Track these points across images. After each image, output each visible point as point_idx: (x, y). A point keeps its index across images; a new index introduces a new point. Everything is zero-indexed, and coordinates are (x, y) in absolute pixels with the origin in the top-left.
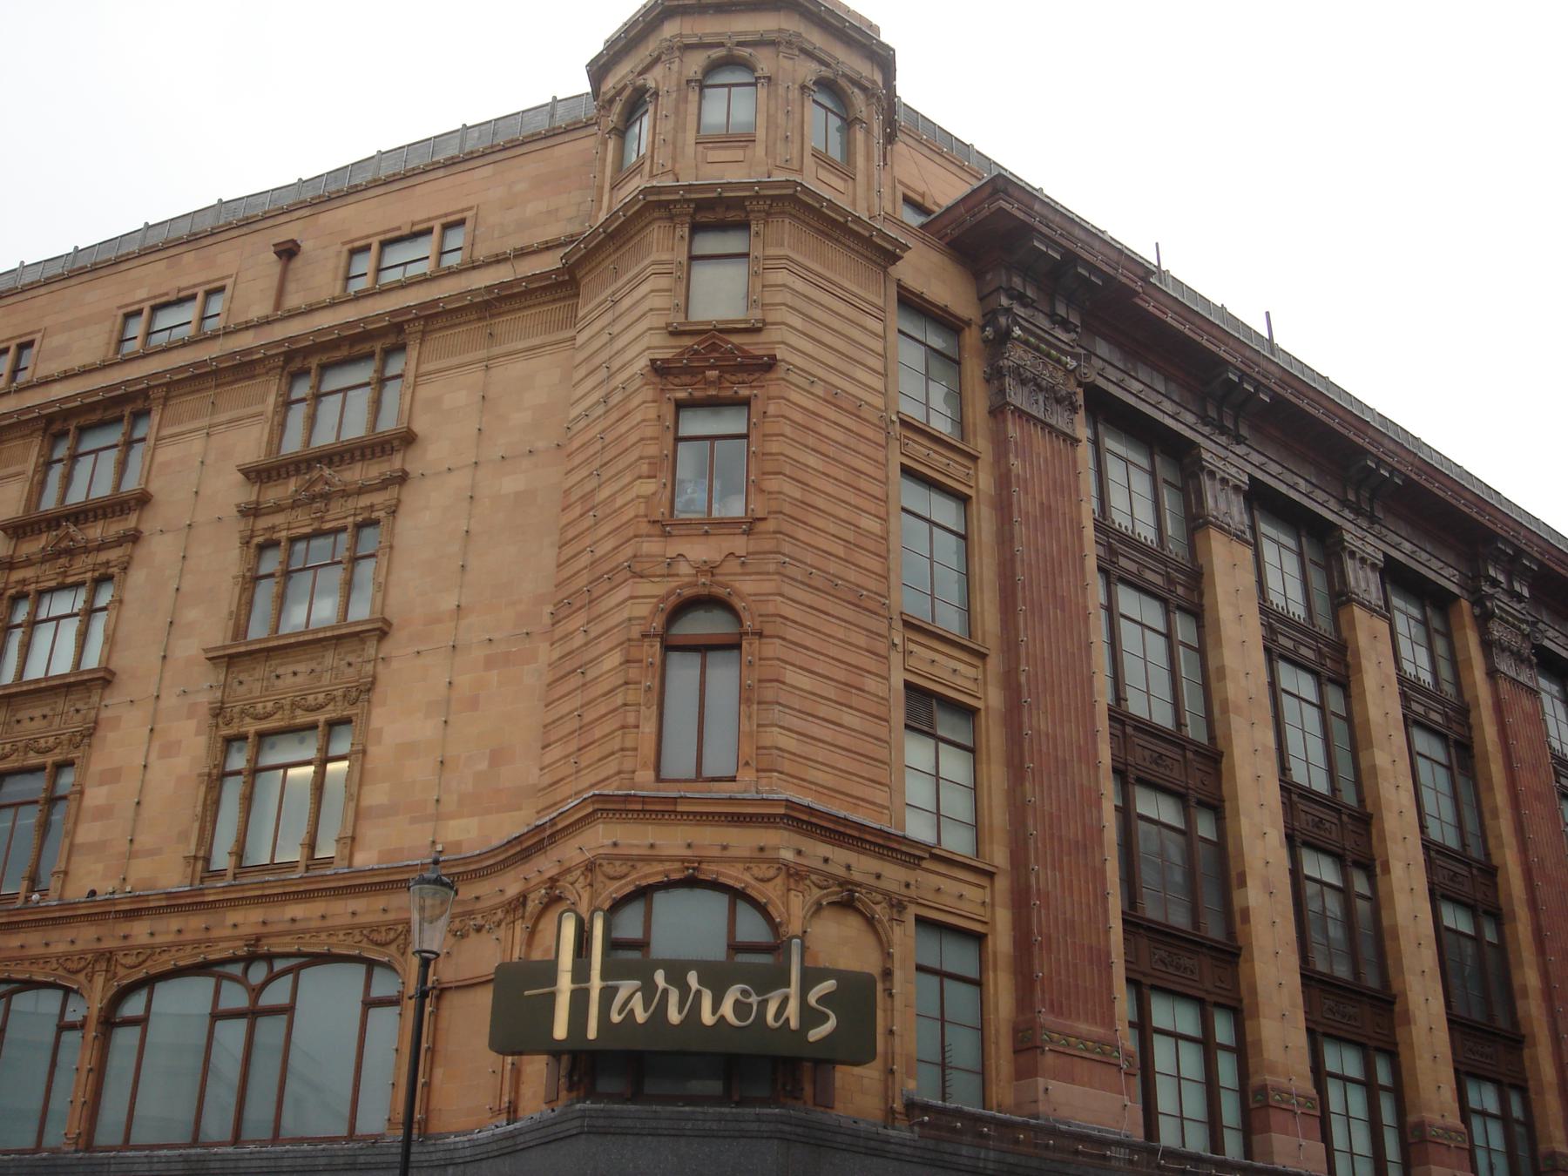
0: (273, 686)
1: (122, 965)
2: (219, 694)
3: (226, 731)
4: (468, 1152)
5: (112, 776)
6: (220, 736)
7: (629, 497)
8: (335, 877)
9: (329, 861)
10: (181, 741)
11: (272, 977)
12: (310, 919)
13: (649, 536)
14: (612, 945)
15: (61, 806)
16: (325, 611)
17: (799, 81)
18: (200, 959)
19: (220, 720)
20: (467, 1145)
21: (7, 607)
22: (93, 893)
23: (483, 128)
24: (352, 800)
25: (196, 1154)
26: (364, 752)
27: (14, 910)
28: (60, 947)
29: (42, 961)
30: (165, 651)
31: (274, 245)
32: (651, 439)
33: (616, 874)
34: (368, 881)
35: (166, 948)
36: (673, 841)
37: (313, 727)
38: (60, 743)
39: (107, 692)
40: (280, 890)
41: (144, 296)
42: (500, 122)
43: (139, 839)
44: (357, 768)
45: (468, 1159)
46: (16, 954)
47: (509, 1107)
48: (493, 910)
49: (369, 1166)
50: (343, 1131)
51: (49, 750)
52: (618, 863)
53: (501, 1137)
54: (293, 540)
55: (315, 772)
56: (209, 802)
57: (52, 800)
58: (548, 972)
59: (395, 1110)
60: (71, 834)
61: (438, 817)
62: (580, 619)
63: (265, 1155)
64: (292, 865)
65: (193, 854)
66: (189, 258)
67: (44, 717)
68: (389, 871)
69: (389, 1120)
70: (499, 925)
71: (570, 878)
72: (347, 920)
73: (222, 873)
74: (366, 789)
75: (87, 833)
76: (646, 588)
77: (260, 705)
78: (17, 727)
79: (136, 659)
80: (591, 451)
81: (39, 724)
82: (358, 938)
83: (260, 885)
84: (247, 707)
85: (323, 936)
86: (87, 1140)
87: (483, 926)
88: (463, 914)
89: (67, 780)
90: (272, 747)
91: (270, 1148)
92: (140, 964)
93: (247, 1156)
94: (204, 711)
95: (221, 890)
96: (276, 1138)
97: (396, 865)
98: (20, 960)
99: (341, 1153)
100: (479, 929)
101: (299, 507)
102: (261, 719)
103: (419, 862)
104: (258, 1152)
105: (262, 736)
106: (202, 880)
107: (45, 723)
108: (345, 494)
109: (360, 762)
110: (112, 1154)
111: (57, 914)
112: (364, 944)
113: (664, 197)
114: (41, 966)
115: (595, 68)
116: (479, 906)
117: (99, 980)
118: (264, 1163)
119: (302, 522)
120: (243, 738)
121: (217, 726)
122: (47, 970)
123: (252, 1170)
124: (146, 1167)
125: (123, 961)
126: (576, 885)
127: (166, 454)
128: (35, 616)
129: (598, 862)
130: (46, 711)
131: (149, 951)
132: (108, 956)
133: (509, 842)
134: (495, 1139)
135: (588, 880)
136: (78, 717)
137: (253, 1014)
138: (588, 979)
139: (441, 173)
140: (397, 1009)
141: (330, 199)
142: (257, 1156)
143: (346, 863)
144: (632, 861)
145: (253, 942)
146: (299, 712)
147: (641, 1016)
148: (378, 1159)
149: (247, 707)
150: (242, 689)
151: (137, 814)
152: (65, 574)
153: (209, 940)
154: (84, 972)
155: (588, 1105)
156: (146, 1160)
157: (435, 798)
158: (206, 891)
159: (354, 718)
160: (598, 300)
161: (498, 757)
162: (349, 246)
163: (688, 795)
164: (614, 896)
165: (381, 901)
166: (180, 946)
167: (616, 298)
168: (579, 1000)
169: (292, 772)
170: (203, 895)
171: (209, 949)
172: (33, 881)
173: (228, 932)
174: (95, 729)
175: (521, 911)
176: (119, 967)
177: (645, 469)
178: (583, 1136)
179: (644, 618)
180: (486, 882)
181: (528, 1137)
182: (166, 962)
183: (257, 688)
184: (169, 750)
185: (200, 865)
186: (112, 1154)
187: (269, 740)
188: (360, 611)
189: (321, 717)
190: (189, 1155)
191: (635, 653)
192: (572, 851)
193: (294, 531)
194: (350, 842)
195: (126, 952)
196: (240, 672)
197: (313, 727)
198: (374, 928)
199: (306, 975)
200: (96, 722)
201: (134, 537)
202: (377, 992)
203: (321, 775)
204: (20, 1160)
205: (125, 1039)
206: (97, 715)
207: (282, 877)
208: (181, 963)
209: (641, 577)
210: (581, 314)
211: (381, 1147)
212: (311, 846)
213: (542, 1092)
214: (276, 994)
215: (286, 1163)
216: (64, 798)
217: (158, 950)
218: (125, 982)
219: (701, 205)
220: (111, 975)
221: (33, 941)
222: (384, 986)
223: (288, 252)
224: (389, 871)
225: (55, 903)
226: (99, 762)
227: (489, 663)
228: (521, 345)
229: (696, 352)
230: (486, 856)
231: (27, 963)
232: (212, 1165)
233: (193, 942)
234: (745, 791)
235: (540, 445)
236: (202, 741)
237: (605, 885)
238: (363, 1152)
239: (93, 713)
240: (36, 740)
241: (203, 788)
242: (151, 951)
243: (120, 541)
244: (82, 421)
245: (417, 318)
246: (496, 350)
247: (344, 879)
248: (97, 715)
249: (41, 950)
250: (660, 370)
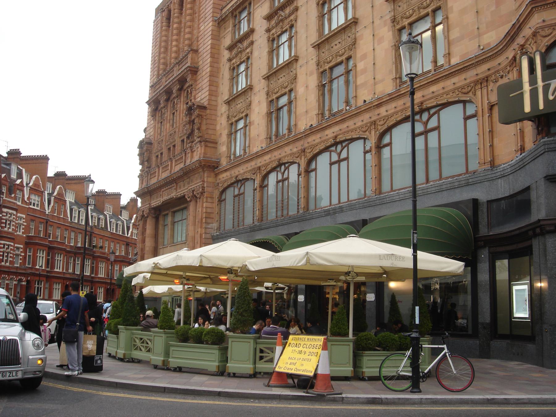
0: (411, 3)
1: (379, 125)
2: (393, 14)
3: (398, 27)
4: (509, 170)
5: (364, 57)
8: (445, 71)
9: (442, 66)
10: (384, 36)
14: (546, 67)
15: (351, 72)
18: (404, 116)
19: (395, 23)
20: (508, 167)
21: (321, 8)
24: (446, 38)
26: (447, 18)
27: (342, 114)
28: (359, 124)
29: (354, 130)
30: (372, 4)
33: (546, 34)
37: (427, 15)
38: (346, 51)
39: (357, 27)
40: (426, 82)
43: (377, 77)
44: (446, 25)
45: (510, 173)
46: (347, 130)
47: (521, 148)
48: (506, 67)
49: (474, 183)
50: (464, 171)
51: (343, 54)
52: (546, 29)
53: (519, 161)
55: (431, 32)
56: (397, 56)
57: (348, 72)
58: (519, 84)
59: (480, 159)
60: (355, 82)
61: (479, 35)
63: (436, 185)
64: (429, 71)
65: (395, 77)
67: (340, 43)
68: (464, 62)
69: (479, 163)
70: (509, 73)
71: (529, 43)
72: (452, 87)
73: (406, 81)
74: (450, 33)
75: (360, 81)
77: (407, 13)
78: (332, 50)
79: (364, 12)
81: (339, 45)
82: (457, 93)
83: (419, 82)
84: (403, 15)
85: (445, 96)
86: (379, 190)
87: (503, 75)
88: (495, 72)
89: (351, 63)
90: (416, 27)
91: (438, 182)
93: (430, 187)
94: (389, 22)
95: (406, 88)
96: (441, 178)
97: (466, 59)
98: (348, 132)
99: (462, 179)
102: (409, 18)
103: (474, 56)
105: (411, 24)
106: (400, 86)
109: (446, 22)
110: (386, 194)
111: (356, 112)
114: (355, 132)
117: (373, 132)
118: (437, 188)
120: (403, 28)
121: (394, 26)
122: (357, 133)
123: (433, 192)
124: (398, 197)
125: (379, 124)
126: (531, 45)
128: (330, 8)
129: (537, 31)
130: (340, 40)
131: (387, 118)
132: (374, 122)
133: (505, 36)
135: (534, 41)
136: (350, 39)
138: (536, 83)
140: (476, 118)
142: (433, 186)
143: (448, 64)
145: (420, 105)
146: (421, 10)
148: (477, 179)
150: (401, 8)
151: (374, 68)
154: (368, 131)
155: (546, 139)
156: (397, 194)
157: (477, 27)
158: (401, 90)
159: (441, 6)
164: (546, 44)
165: (463, 76)
166: (396, 113)
168: (534, 93)
170: (400, 91)
171: (406, 111)
172: (347, 102)
174: (355, 41)
175: (514, 64)
176: (378, 126)
178: (546, 153)
180: (502, 56)
181: (527, 159)
183: (405, 6)
184: (381, 40)
185: (398, 81)
186: (386, 194)
187: (414, 25)
189: (429, 10)
192: (527, 32)
194: (448, 55)
195: (380, 120)
196: (398, 3)
197: (427, 15)
199: (442, 113)
200: (355, 39)
202: (469, 113)
204: (359, 202)
205: (386, 152)
206: (355, 36)
207: (426, 77)
208: (398, 119)
211: (477, 174)
212: (435, 61)
213: (532, 139)
214: (433, 123)
215: (444, 187)
216: (351, 70)
217: (390, 116)
218: (382, 131)
221: (350, 124)
222: (470, 110)
224: (464, 62)
225: (354, 108)
230: (499, 45)
231: (350, 132)
236: (391, 33)
237: (542, 41)
238: (470, 178)
239: (354, 35)
240: (338, 52)
241: (394, 51)
242: (388, 117)
247: (448, 71)
248: (355, 36)
249: (353, 127)
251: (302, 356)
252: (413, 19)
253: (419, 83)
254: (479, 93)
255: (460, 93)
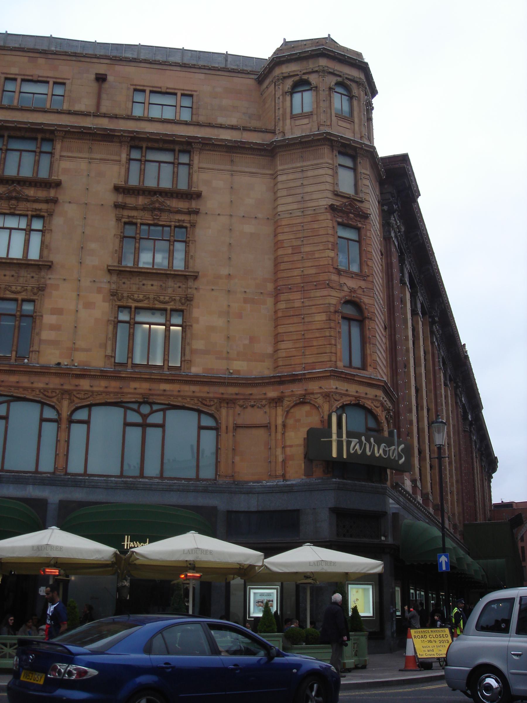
6: (116, 305)
7: (323, 255)
11: (152, 412)
12: (173, 391)
13: (334, 273)
16: (161, 259)
17: (328, 87)
22: (59, 364)
23: (193, 53)
25: (130, 481)
28: (41, 385)
31: (96, 74)
32: (331, 235)
34: (202, 380)
35: (99, 393)
36: (353, 389)
40: (159, 377)
41: (17, 72)
42: (201, 53)
51: (19, 293)
54: (142, 224)
62: (297, 296)
63: (165, 484)
66: (41, 61)
67: (13, 276)
72: (190, 394)
75: (45, 335)
76: (334, 293)
80: (295, 229)
87: (255, 405)
92: (87, 398)
98: (18, 388)
99: (200, 485)
100: (253, 406)
101: (145, 210)
104: (161, 482)
105: (137, 308)
107: (12, 279)
108: (170, 211)
111: (39, 370)
112: (200, 404)
113: (332, 138)
115: (278, 60)
116: (251, 397)
117: (65, 403)
119: (147, 217)
125: (78, 396)
127: (65, 164)
131: (90, 394)
134: (277, 486)
137: (144, 426)
139: (179, 69)
141: (121, 60)
144: (342, 395)
146: (156, 302)
147: (359, 452)
149: (130, 295)
150: (125, 286)
152: (15, 209)
153: (123, 393)
160: (294, 165)
161: (252, 339)
162: (134, 87)
163: (359, 374)
165: (206, 389)
166: (108, 393)
167: (304, 169)
169: (152, 326)
170: (120, 373)
173: (132, 391)
177: (330, 246)
179: (335, 305)
182: (99, 399)
183: (134, 288)
184: (89, 305)
188: (179, 264)
190: (127, 481)
191: (332, 317)
193: (143, 221)
198: (204, 399)
201: (55, 201)
202: (203, 424)
203: (167, 330)
209: (332, 288)
210: (280, 168)
215: (175, 487)
219: (344, 145)
220: (71, 401)
221: (25, 380)
223: (101, 79)
226: (48, 304)
227: (246, 301)
228: (247, 170)
229: (345, 205)
232: (139, 486)
233: (114, 393)
234: (370, 375)
235: (260, 216)
240: (10, 286)
243: (47, 201)
244: (12, 133)
245: (200, 143)
246: (235, 168)
250: (332, 208)
251: (434, 644)
252: (142, 305)
253: (149, 375)
254: (224, 411)
255: (200, 403)
